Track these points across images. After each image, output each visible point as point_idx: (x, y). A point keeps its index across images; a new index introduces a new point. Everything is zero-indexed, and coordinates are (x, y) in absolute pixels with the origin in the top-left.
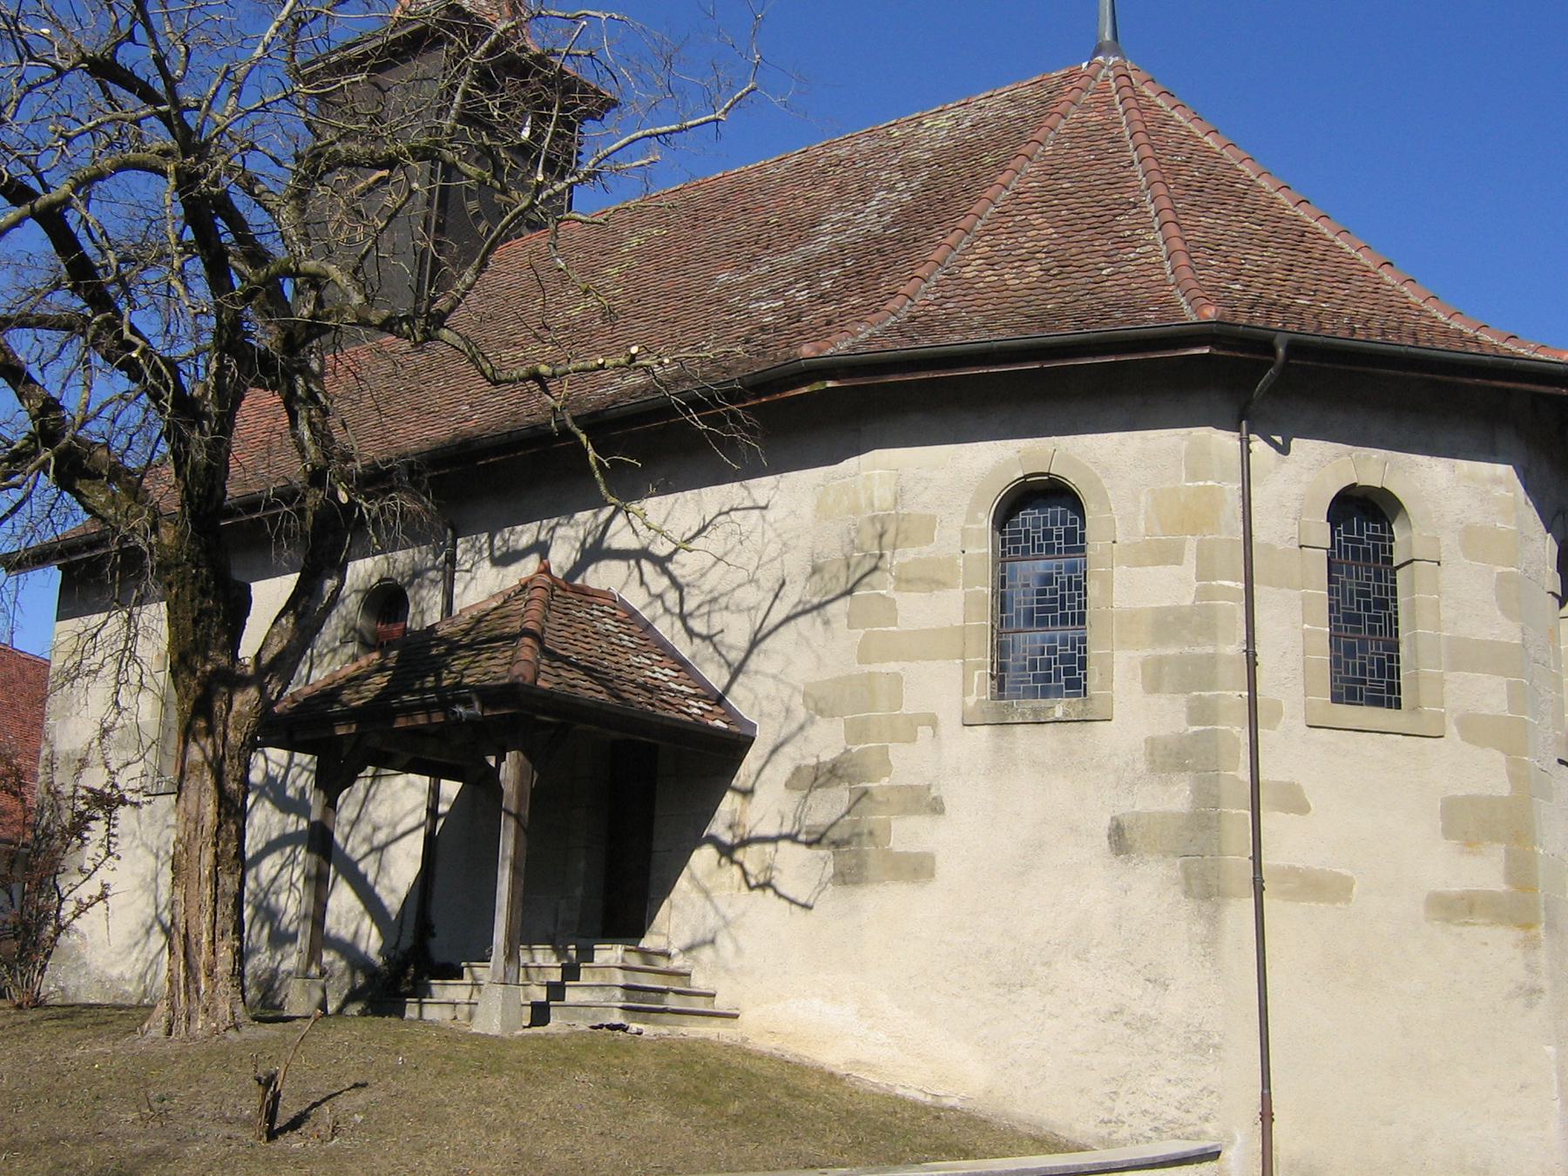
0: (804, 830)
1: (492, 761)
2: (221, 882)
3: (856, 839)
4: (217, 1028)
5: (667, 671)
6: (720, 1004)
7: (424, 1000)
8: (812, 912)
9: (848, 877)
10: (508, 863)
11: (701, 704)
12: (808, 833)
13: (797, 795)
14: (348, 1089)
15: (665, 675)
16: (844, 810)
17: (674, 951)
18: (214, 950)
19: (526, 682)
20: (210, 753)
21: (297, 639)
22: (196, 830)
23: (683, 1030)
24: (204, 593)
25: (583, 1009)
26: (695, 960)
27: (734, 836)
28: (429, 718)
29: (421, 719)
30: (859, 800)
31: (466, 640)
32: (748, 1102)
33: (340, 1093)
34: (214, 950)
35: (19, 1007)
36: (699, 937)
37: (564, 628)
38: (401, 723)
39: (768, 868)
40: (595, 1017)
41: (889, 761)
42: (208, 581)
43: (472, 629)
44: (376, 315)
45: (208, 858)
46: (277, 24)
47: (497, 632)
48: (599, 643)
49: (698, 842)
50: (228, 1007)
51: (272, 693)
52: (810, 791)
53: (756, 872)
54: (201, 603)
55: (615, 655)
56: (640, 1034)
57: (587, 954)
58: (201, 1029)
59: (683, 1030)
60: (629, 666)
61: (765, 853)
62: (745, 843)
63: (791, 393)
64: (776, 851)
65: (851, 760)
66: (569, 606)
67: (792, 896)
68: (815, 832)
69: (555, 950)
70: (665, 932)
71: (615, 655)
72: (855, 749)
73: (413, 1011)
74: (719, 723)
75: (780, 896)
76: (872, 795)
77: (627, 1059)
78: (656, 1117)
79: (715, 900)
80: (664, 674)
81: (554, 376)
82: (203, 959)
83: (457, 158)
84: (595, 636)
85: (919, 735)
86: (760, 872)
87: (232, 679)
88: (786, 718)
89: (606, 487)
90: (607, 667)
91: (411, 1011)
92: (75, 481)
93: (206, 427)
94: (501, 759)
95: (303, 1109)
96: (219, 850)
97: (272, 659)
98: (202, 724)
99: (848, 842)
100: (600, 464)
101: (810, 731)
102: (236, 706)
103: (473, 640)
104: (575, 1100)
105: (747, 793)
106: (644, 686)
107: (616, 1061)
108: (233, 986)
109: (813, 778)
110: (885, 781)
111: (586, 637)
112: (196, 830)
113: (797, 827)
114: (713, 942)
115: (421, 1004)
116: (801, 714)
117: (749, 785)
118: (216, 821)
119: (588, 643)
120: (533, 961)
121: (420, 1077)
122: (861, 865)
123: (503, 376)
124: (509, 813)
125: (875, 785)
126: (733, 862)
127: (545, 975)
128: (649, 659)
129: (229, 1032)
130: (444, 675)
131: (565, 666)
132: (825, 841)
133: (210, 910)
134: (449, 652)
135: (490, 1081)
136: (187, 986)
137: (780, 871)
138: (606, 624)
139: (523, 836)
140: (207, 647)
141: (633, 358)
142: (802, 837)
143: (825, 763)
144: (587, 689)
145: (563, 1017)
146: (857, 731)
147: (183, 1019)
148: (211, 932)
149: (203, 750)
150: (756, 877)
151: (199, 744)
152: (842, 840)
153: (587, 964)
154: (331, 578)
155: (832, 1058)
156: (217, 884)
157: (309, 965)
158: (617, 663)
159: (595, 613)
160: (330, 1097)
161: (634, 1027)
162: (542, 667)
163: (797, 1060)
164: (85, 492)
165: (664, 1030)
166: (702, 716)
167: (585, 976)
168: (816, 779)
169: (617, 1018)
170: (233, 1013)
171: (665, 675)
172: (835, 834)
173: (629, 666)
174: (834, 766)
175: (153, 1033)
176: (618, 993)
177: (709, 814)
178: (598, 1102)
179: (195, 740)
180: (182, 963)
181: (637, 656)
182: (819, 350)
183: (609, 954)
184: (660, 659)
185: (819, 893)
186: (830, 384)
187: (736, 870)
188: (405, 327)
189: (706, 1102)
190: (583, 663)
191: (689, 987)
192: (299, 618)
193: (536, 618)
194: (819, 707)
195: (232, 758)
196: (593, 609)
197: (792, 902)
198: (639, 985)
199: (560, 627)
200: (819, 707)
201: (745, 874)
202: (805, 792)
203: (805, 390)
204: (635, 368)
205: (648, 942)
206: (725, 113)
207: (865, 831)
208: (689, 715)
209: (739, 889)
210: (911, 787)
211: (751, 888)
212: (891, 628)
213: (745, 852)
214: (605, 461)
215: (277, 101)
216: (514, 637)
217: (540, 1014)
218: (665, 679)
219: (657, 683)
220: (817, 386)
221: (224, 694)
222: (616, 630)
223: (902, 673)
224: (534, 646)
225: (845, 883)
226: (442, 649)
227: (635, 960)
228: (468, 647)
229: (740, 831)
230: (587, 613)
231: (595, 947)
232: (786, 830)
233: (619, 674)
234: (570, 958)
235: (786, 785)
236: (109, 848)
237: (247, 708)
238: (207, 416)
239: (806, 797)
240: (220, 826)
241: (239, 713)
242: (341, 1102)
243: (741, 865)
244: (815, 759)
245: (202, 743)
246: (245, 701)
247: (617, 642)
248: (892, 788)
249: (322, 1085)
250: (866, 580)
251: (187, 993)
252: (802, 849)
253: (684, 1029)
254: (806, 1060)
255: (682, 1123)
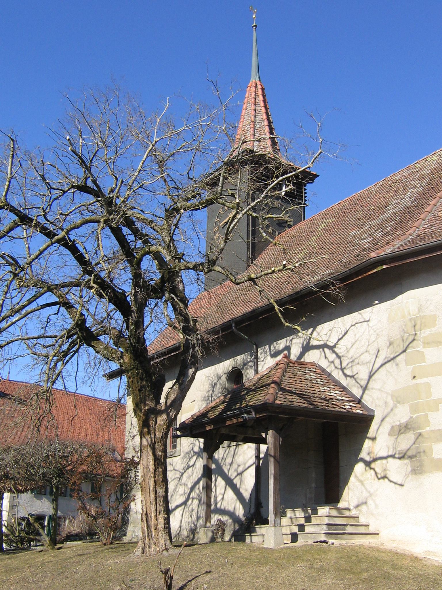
0: (397, 452)
1: (264, 435)
2: (158, 492)
3: (418, 454)
4: (159, 551)
5: (337, 392)
6: (372, 529)
7: (252, 534)
8: (404, 487)
9: (417, 471)
10: (272, 476)
11: (351, 404)
12: (399, 454)
13: (393, 438)
14: (204, 574)
15: (336, 394)
16: (412, 442)
17: (351, 508)
18: (157, 519)
19: (270, 402)
20: (149, 441)
21: (180, 394)
22: (147, 472)
23: (353, 541)
24: (142, 379)
25: (310, 535)
26: (360, 511)
27: (370, 458)
28: (238, 420)
29: (235, 421)
30: (418, 438)
31: (254, 388)
32: (372, 572)
33: (200, 576)
34: (157, 519)
35: (105, 544)
36: (360, 502)
37: (291, 379)
38: (228, 423)
39: (385, 470)
40: (314, 538)
41: (429, 420)
42: (143, 375)
43: (257, 383)
44: (191, 265)
45: (152, 482)
46: (142, 162)
47: (264, 383)
48: (307, 383)
49: (357, 461)
50: (163, 542)
51: (172, 416)
52: (398, 436)
53: (380, 472)
54: (141, 383)
55: (313, 388)
56: (333, 544)
57: (315, 511)
58: (153, 551)
59: (353, 541)
60: (319, 391)
61: (383, 464)
62: (375, 460)
63: (370, 273)
64: (387, 462)
65: (412, 421)
66: (295, 370)
67: (395, 481)
68: (402, 453)
69: (303, 510)
70: (347, 500)
71: (313, 388)
72: (414, 416)
73: (248, 539)
74: (358, 411)
75: (391, 481)
76: (423, 435)
77: (323, 556)
78: (329, 581)
79: (365, 485)
80: (335, 393)
81: (257, 278)
82: (153, 522)
83: (224, 201)
84: (306, 381)
85: (440, 407)
86: (382, 471)
87: (157, 412)
88: (386, 406)
89: (284, 319)
90: (309, 393)
91: (248, 540)
92: (91, 342)
93: (133, 316)
94: (267, 434)
95: (185, 583)
96: (156, 479)
97: (171, 402)
98: (146, 430)
99: (415, 456)
100: (280, 311)
101: (396, 411)
102: (158, 422)
103: (256, 387)
104: (295, 575)
105: (374, 439)
106: (325, 399)
107: (318, 557)
108: (165, 533)
109: (399, 430)
110: (428, 429)
111: (301, 381)
112: (147, 472)
113: (394, 452)
114: (366, 503)
115: (251, 536)
116: (391, 404)
117: (374, 436)
118: (154, 468)
119: (302, 384)
120: (295, 515)
121: (233, 567)
122: (421, 466)
123: (239, 281)
124: (271, 456)
125: (424, 430)
126: (371, 468)
127: (298, 521)
128: (329, 388)
129: (164, 552)
130: (243, 402)
131: (289, 394)
132: (406, 457)
133: (154, 503)
134: (247, 393)
135: (261, 568)
136: (148, 534)
137: (390, 471)
138: (311, 375)
139: (277, 465)
140: (145, 400)
141: (284, 266)
142: (397, 456)
143: (403, 423)
144: (298, 402)
145: (303, 539)
146: (414, 409)
147: (148, 547)
148: (155, 512)
149: (147, 440)
150: (380, 474)
151: (146, 438)
152: (413, 455)
153: (313, 516)
154: (191, 369)
155: (418, 550)
156: (156, 493)
157: (206, 523)
158: (314, 391)
159: (307, 371)
160: (196, 577)
161: (330, 541)
162: (279, 395)
163: (402, 552)
164: (95, 346)
165: (343, 542)
166: (351, 409)
167: (314, 521)
168: (400, 430)
169: (323, 538)
170: (165, 544)
171: (336, 394)
172: (410, 453)
173: (319, 391)
174: (407, 424)
175: (137, 553)
176: (325, 527)
177: (360, 450)
178: (305, 575)
179: (144, 437)
180: (146, 525)
181: (323, 387)
182: (378, 254)
183: (324, 511)
184: (334, 387)
185: (406, 479)
186: (384, 267)
187: (372, 471)
188: (201, 267)
189: (353, 573)
190: (298, 392)
191: (359, 522)
192: (180, 385)
193: (278, 376)
194: (398, 400)
195: (158, 442)
196: (306, 370)
197: (395, 483)
198: (336, 523)
199: (290, 379)
200: (398, 400)
201: (376, 473)
202: (396, 436)
203: (375, 271)
204: (286, 270)
205: (341, 505)
206: (312, 164)
207: (422, 451)
208: (345, 409)
209: (374, 479)
210: (439, 430)
211: (379, 479)
212: (423, 364)
213: (375, 464)
214: (281, 309)
215: (138, 189)
216: (269, 385)
217: (294, 537)
218: (335, 395)
219: (331, 397)
220: (379, 268)
221: (153, 418)
222: (315, 377)
223: (430, 382)
224: (276, 387)
225: (416, 474)
226: (245, 392)
227: (334, 513)
228: (254, 390)
229: (372, 455)
230: (303, 372)
231: (318, 508)
232: (390, 453)
233: (314, 395)
234: (309, 513)
235: (389, 434)
236: (136, 481)
237: (163, 422)
238: (133, 311)
239: (397, 438)
240: (155, 470)
241: (160, 424)
242: (200, 579)
243: (374, 469)
244: (399, 422)
245: (147, 437)
246: (162, 419)
247: (316, 382)
248: (431, 431)
249: (194, 573)
250: (410, 345)
251: (148, 537)
252: (397, 461)
253: (354, 541)
254: (407, 551)
255: (340, 583)
